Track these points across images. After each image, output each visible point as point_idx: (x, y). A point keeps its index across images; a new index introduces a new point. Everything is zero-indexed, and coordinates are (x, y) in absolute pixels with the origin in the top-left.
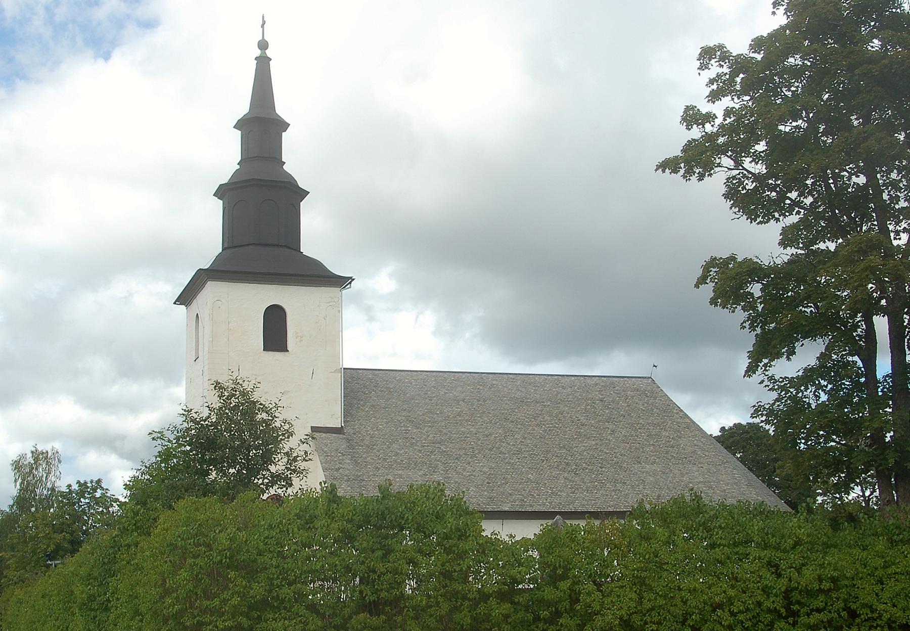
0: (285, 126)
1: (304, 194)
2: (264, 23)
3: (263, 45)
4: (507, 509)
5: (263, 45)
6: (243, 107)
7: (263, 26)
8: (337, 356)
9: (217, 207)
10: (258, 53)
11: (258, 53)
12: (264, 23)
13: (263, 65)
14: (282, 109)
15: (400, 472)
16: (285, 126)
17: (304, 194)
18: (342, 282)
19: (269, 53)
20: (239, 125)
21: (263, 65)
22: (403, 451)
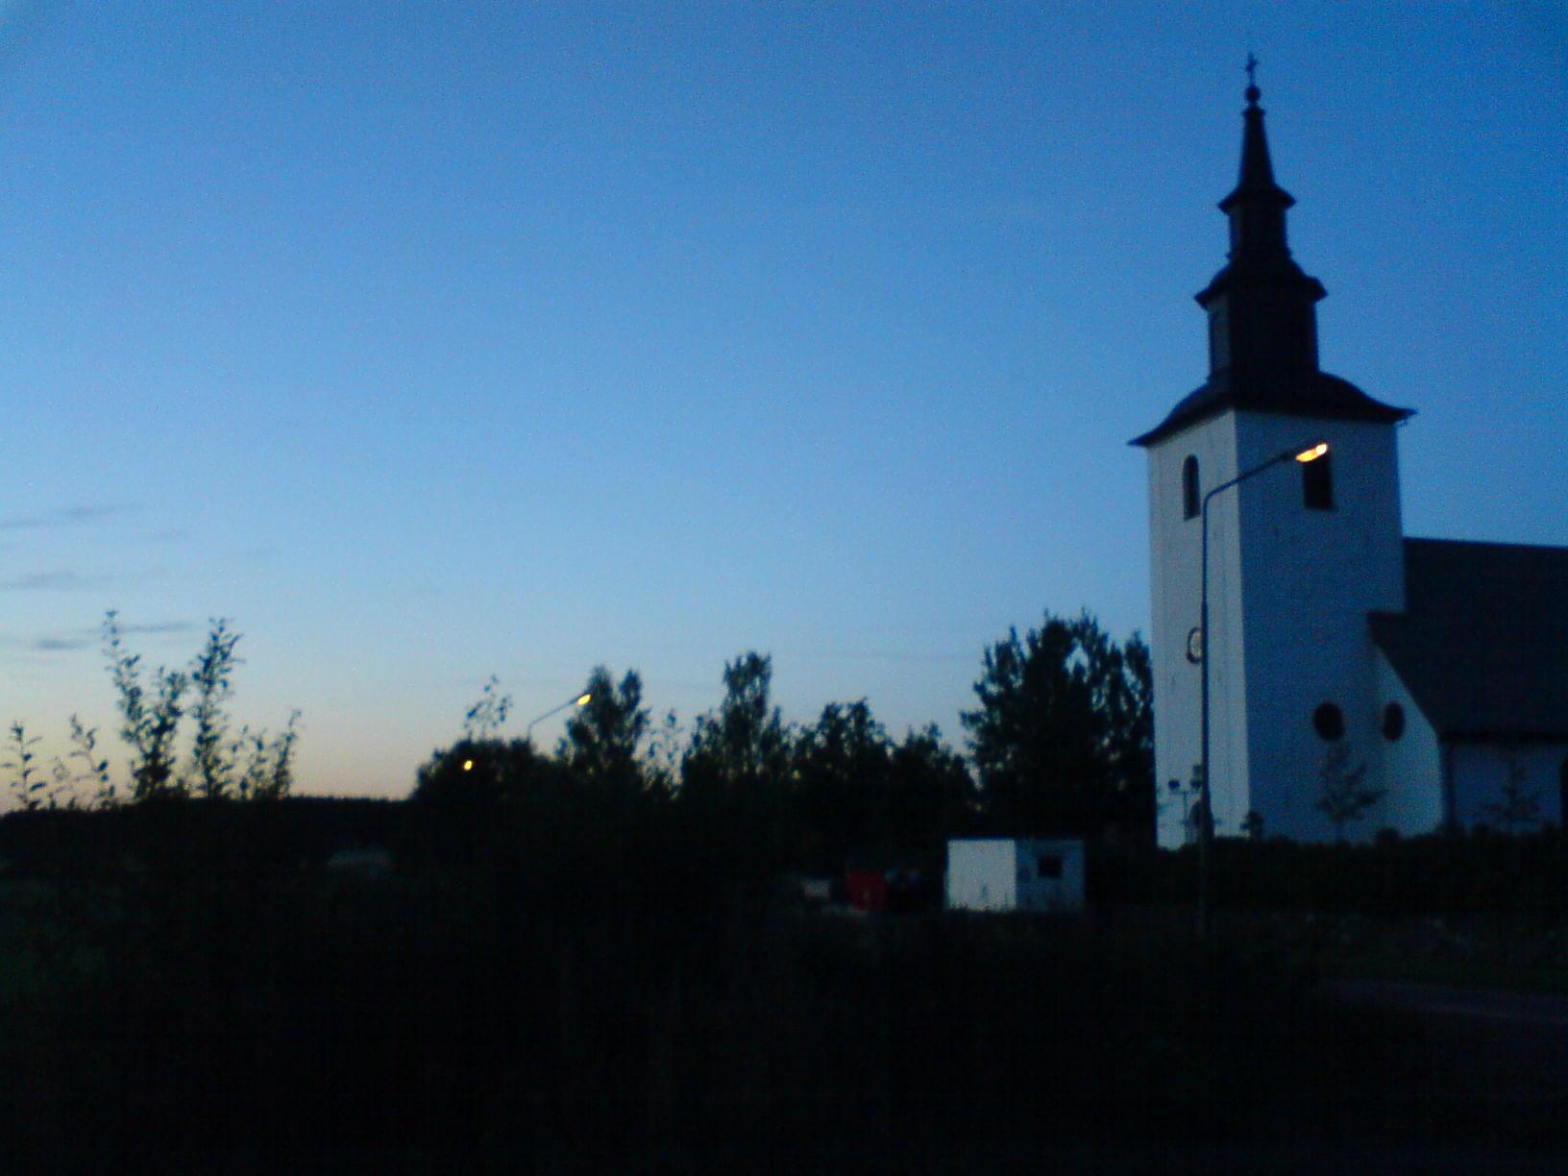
0: (1287, 201)
3: (1253, 94)
5: (1253, 94)
9: (1201, 318)
11: (1245, 105)
13: (1254, 120)
14: (1284, 177)
16: (1287, 201)
20: (1225, 206)
21: (1254, 120)
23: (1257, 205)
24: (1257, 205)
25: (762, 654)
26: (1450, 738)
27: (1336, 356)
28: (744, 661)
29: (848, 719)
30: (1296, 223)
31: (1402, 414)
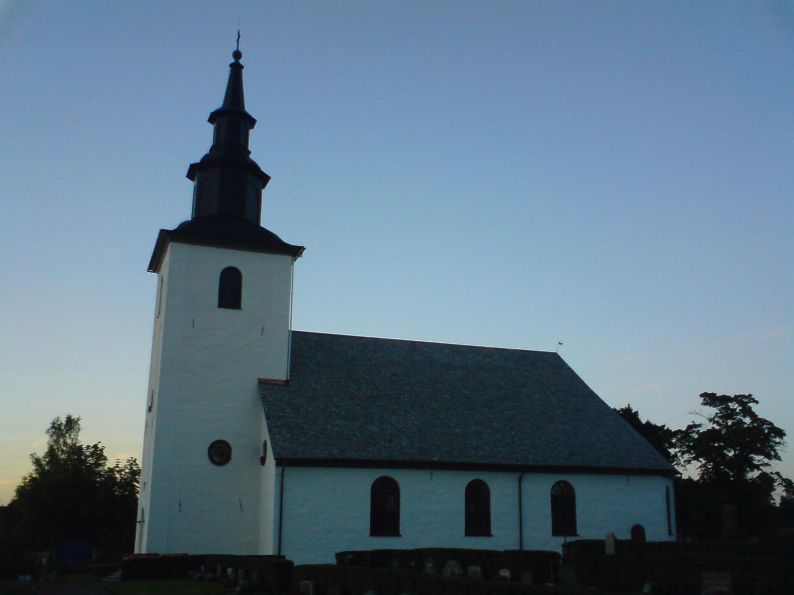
0: (252, 122)
1: (265, 179)
2: (239, 37)
3: (237, 55)
4: (436, 459)
5: (237, 55)
6: (218, 102)
7: (238, 41)
8: (285, 316)
10: (233, 61)
11: (233, 61)
12: (239, 37)
13: (236, 70)
14: (250, 107)
15: (338, 422)
17: (265, 179)
18: (296, 251)
19: (241, 61)
21: (236, 70)
22: (342, 404)
23: (232, 120)
24: (232, 120)
25: (74, 416)
26: (280, 462)
27: (274, 216)
28: (63, 420)
29: (89, 456)
30: (254, 135)
31: (296, 251)
